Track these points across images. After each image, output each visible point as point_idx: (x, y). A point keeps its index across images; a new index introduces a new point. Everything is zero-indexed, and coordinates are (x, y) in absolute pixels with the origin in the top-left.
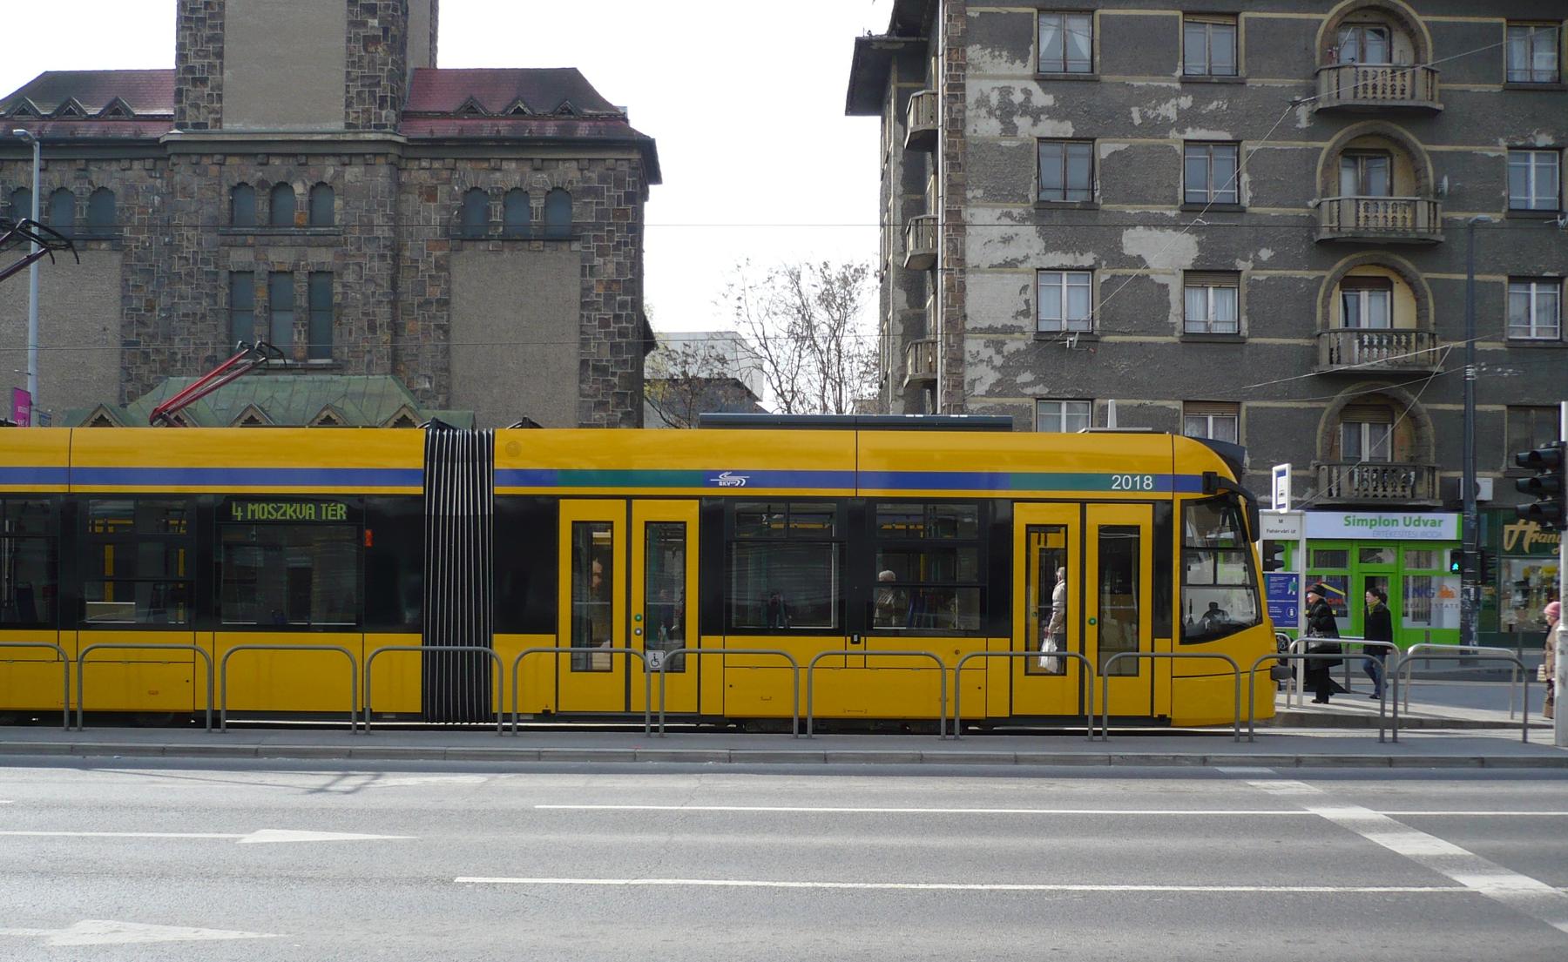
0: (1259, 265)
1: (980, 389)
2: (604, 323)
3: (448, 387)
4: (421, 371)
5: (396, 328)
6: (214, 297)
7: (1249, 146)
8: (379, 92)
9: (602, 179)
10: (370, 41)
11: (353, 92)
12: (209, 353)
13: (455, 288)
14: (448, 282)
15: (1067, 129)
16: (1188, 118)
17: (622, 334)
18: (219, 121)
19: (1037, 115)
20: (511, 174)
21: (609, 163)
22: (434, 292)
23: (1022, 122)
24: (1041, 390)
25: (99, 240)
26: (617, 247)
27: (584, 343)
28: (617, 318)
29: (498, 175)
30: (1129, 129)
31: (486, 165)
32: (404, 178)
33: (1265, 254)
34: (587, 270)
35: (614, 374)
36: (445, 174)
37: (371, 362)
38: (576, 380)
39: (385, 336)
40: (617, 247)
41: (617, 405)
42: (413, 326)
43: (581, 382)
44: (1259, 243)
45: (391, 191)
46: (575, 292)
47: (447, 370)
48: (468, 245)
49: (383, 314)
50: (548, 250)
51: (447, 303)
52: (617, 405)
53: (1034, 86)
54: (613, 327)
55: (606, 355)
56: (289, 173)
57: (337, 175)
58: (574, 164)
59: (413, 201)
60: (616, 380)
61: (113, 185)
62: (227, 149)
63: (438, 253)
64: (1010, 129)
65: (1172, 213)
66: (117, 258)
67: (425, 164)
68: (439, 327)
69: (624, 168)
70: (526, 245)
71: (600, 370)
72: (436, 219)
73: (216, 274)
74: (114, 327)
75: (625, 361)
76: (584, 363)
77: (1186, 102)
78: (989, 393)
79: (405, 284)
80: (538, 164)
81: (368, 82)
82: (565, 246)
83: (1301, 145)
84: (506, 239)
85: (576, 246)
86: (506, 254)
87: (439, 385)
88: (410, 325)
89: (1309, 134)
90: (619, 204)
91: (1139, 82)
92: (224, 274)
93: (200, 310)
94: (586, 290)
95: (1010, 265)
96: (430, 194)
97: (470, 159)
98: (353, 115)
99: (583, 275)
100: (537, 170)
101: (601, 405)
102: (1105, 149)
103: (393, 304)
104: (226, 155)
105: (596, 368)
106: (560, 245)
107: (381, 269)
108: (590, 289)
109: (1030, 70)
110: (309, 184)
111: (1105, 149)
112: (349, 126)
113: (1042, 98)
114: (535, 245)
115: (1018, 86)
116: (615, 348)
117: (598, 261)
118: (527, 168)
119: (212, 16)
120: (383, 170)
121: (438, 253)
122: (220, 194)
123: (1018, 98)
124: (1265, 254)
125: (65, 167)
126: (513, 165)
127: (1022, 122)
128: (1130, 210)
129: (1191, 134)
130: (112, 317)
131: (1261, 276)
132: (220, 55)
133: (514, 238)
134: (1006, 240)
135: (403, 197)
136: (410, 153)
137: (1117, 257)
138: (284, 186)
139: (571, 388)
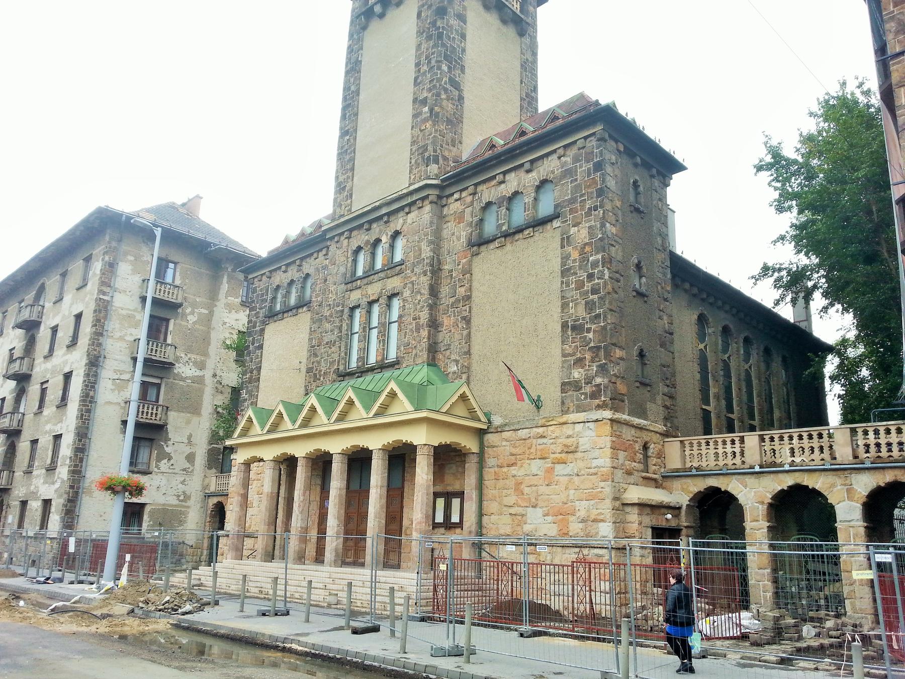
2: (580, 285)
3: (468, 368)
4: (453, 357)
5: (434, 325)
6: (340, 328)
8: (427, 154)
9: (576, 159)
10: (425, 120)
11: (413, 161)
12: (336, 367)
13: (475, 284)
14: (471, 281)
17: (594, 291)
18: (350, 210)
20: (513, 182)
21: (580, 143)
22: (461, 291)
25: (302, 306)
26: (588, 214)
27: (564, 306)
28: (591, 277)
29: (503, 186)
31: (494, 182)
32: (445, 211)
34: (566, 240)
35: (589, 330)
36: (469, 199)
37: (416, 355)
38: (558, 340)
39: (424, 333)
40: (588, 214)
41: (592, 361)
42: (447, 321)
43: (563, 342)
45: (431, 223)
46: (556, 264)
47: (469, 353)
48: (483, 248)
49: (424, 316)
50: (537, 234)
51: (468, 298)
52: (592, 361)
54: (588, 286)
55: (581, 312)
56: (380, 231)
57: (405, 222)
58: (555, 156)
59: (450, 228)
60: (591, 335)
61: (311, 271)
62: (349, 227)
63: (464, 261)
66: (309, 314)
67: (456, 196)
68: (464, 318)
69: (592, 142)
70: (521, 236)
71: (577, 328)
72: (464, 234)
73: (342, 311)
74: (304, 361)
75: (598, 316)
76: (564, 326)
79: (445, 290)
80: (527, 166)
81: (420, 151)
82: (549, 226)
84: (506, 235)
85: (556, 223)
86: (509, 247)
87: (463, 366)
88: (446, 322)
90: (589, 175)
92: (346, 310)
93: (333, 338)
94: (565, 258)
96: (460, 217)
97: (484, 182)
98: (413, 177)
99: (562, 247)
100: (528, 171)
101: (579, 362)
103: (433, 307)
104: (351, 230)
105: (574, 328)
106: (545, 226)
107: (424, 282)
108: (569, 255)
110: (390, 234)
114: (526, 232)
116: (590, 306)
117: (573, 230)
118: (521, 173)
119: (350, 147)
120: (428, 208)
121: (464, 261)
122: (348, 258)
125: (292, 267)
126: (513, 174)
130: (304, 354)
132: (353, 169)
135: (445, 226)
136: (448, 192)
139: (556, 349)
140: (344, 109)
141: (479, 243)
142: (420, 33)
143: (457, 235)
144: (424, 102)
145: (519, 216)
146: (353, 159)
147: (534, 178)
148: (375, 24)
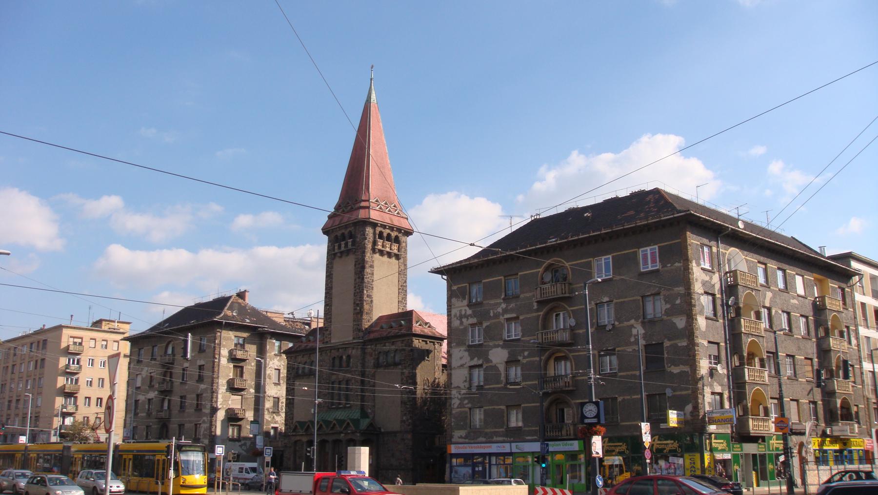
0: (524, 357)
1: (456, 406)
7: (521, 318)
10: (358, 313)
15: (473, 320)
16: (505, 311)
19: (467, 317)
20: (387, 347)
23: (464, 320)
24: (469, 405)
30: (490, 318)
33: (526, 353)
44: (524, 351)
53: (467, 308)
64: (462, 323)
65: (501, 343)
77: (504, 306)
78: (458, 408)
83: (535, 314)
89: (537, 310)
91: (492, 302)
95: (462, 366)
96: (371, 356)
102: (485, 325)
109: (465, 302)
111: (485, 325)
112: (354, 338)
113: (469, 312)
115: (463, 309)
123: (463, 313)
124: (526, 353)
127: (464, 320)
128: (491, 344)
129: (506, 316)
131: (525, 361)
133: (388, 366)
134: (461, 358)
137: (488, 361)
138: (342, 357)
140: (326, 293)
141: (377, 365)
142: (356, 273)
143: (370, 361)
144: (358, 305)
145: (390, 360)
146: (330, 318)
147: (393, 347)
148: (337, 259)
